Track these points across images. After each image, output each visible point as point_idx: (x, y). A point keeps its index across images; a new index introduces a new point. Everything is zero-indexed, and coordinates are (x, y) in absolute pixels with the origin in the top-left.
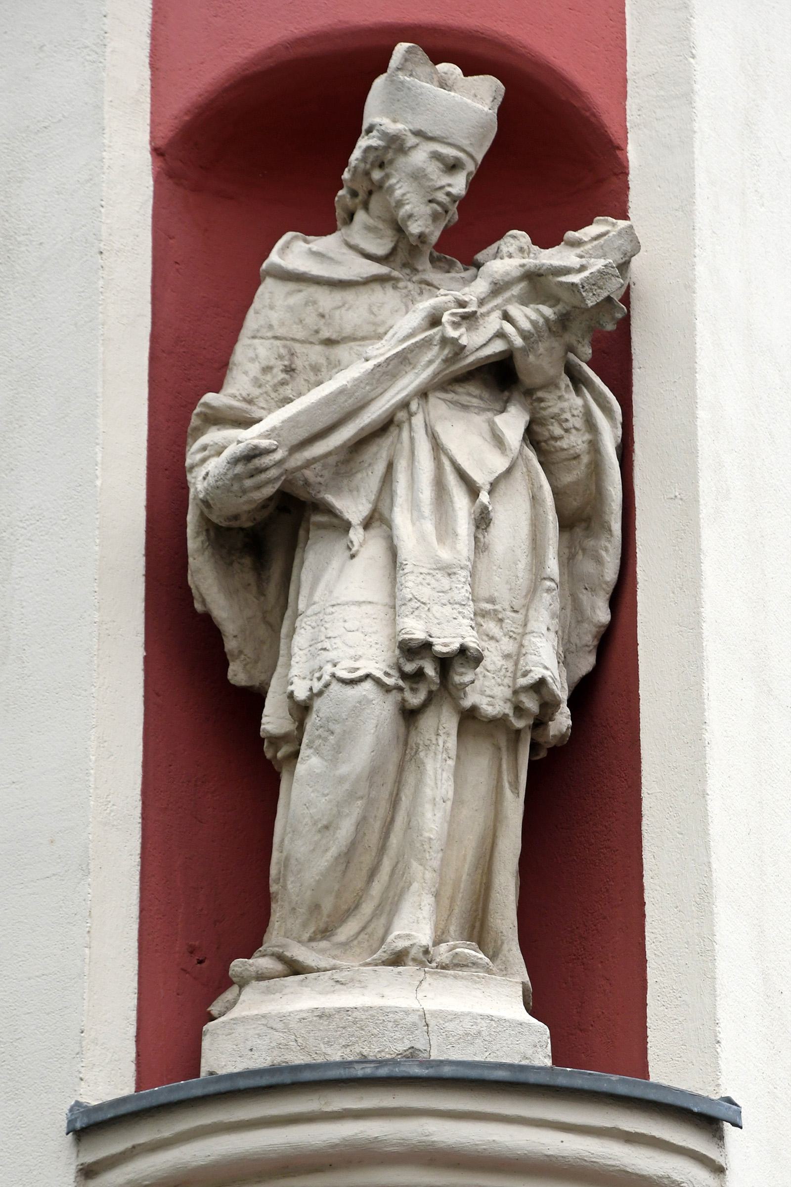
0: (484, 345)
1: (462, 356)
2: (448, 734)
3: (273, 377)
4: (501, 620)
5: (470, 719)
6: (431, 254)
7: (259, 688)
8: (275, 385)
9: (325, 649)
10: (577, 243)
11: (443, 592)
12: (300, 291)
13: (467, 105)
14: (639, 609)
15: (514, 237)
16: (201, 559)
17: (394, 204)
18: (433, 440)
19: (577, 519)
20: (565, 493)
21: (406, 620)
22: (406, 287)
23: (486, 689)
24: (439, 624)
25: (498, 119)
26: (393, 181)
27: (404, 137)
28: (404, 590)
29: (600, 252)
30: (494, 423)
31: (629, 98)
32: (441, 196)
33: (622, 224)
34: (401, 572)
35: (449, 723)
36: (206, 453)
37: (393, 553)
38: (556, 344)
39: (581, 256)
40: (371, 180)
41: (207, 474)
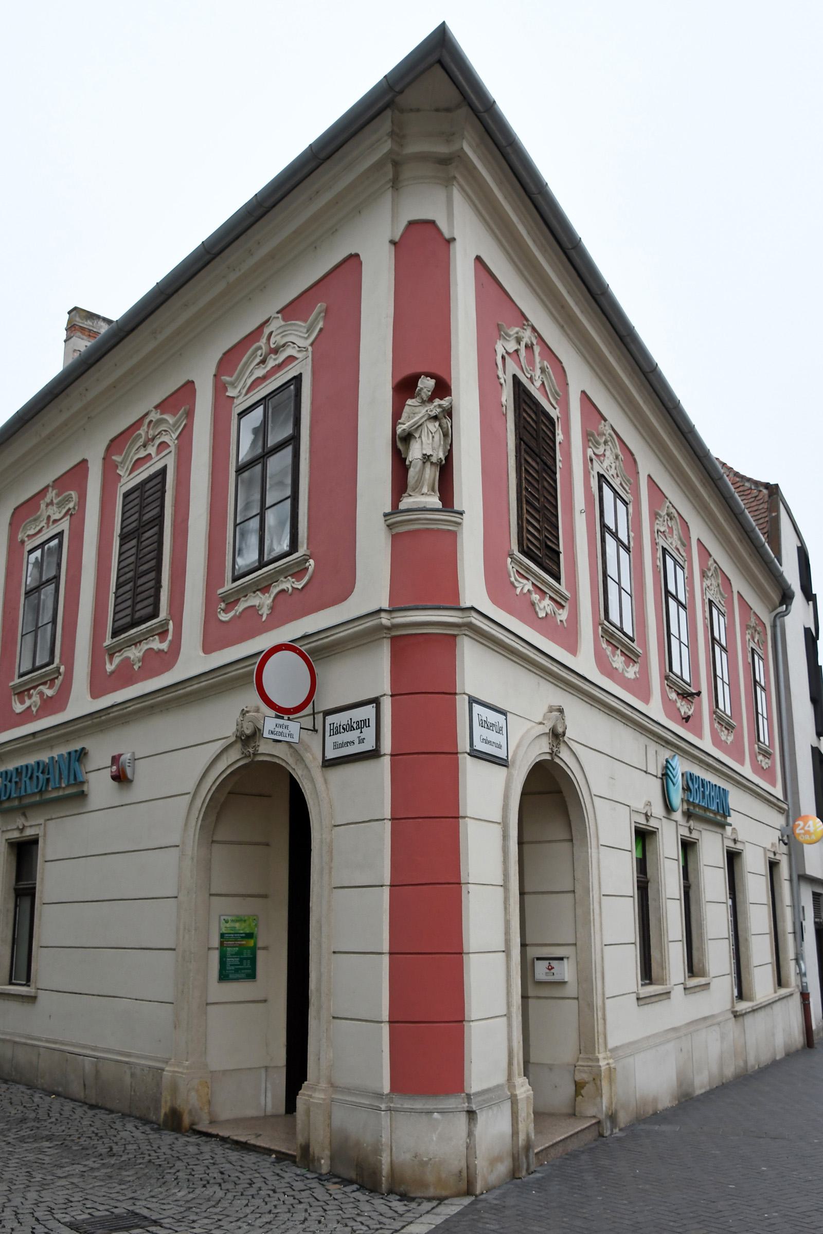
5: (432, 463)
19: (445, 435)
39: (445, 402)
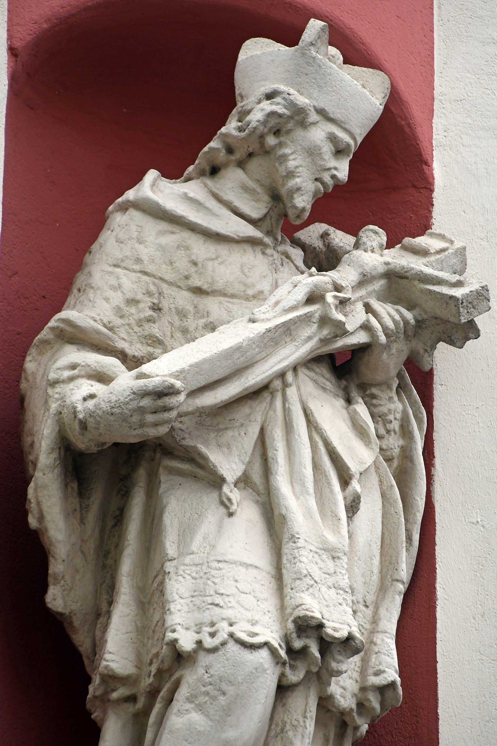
8: (140, 320)
26: (287, 151)
27: (308, 112)
32: (327, 177)
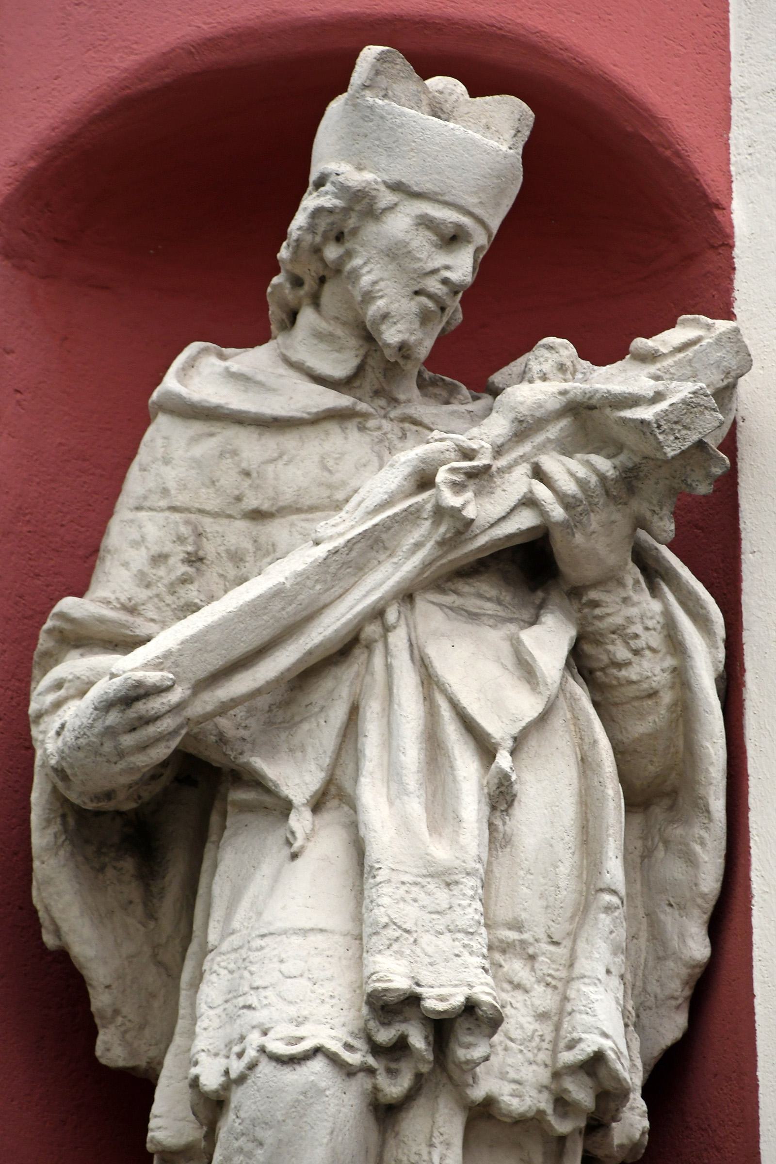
0: (503, 518)
1: (468, 535)
2: (448, 1145)
3: (170, 571)
4: (532, 958)
6: (420, 374)
7: (146, 1071)
8: (172, 584)
9: (249, 1007)
10: (651, 357)
11: (438, 913)
12: (212, 435)
13: (474, 142)
14: (756, 938)
15: (550, 348)
16: (52, 862)
17: (360, 298)
18: (423, 670)
19: (653, 793)
20: (635, 751)
21: (379, 958)
22: (379, 428)
23: (508, 1069)
24: (431, 964)
25: (524, 164)
26: (357, 262)
27: (374, 193)
28: (376, 911)
29: (688, 371)
30: (519, 641)
31: (733, 127)
32: (434, 285)
33: (722, 325)
34: (371, 881)
35: (450, 1125)
36: (62, 693)
37: (358, 849)
38: (617, 516)
39: (656, 378)
40: (322, 260)
41: (63, 726)
